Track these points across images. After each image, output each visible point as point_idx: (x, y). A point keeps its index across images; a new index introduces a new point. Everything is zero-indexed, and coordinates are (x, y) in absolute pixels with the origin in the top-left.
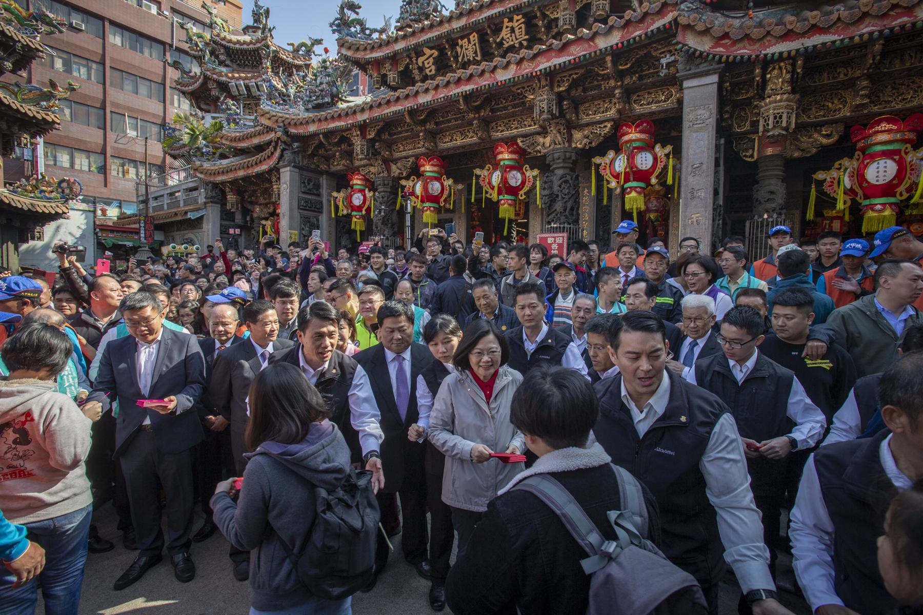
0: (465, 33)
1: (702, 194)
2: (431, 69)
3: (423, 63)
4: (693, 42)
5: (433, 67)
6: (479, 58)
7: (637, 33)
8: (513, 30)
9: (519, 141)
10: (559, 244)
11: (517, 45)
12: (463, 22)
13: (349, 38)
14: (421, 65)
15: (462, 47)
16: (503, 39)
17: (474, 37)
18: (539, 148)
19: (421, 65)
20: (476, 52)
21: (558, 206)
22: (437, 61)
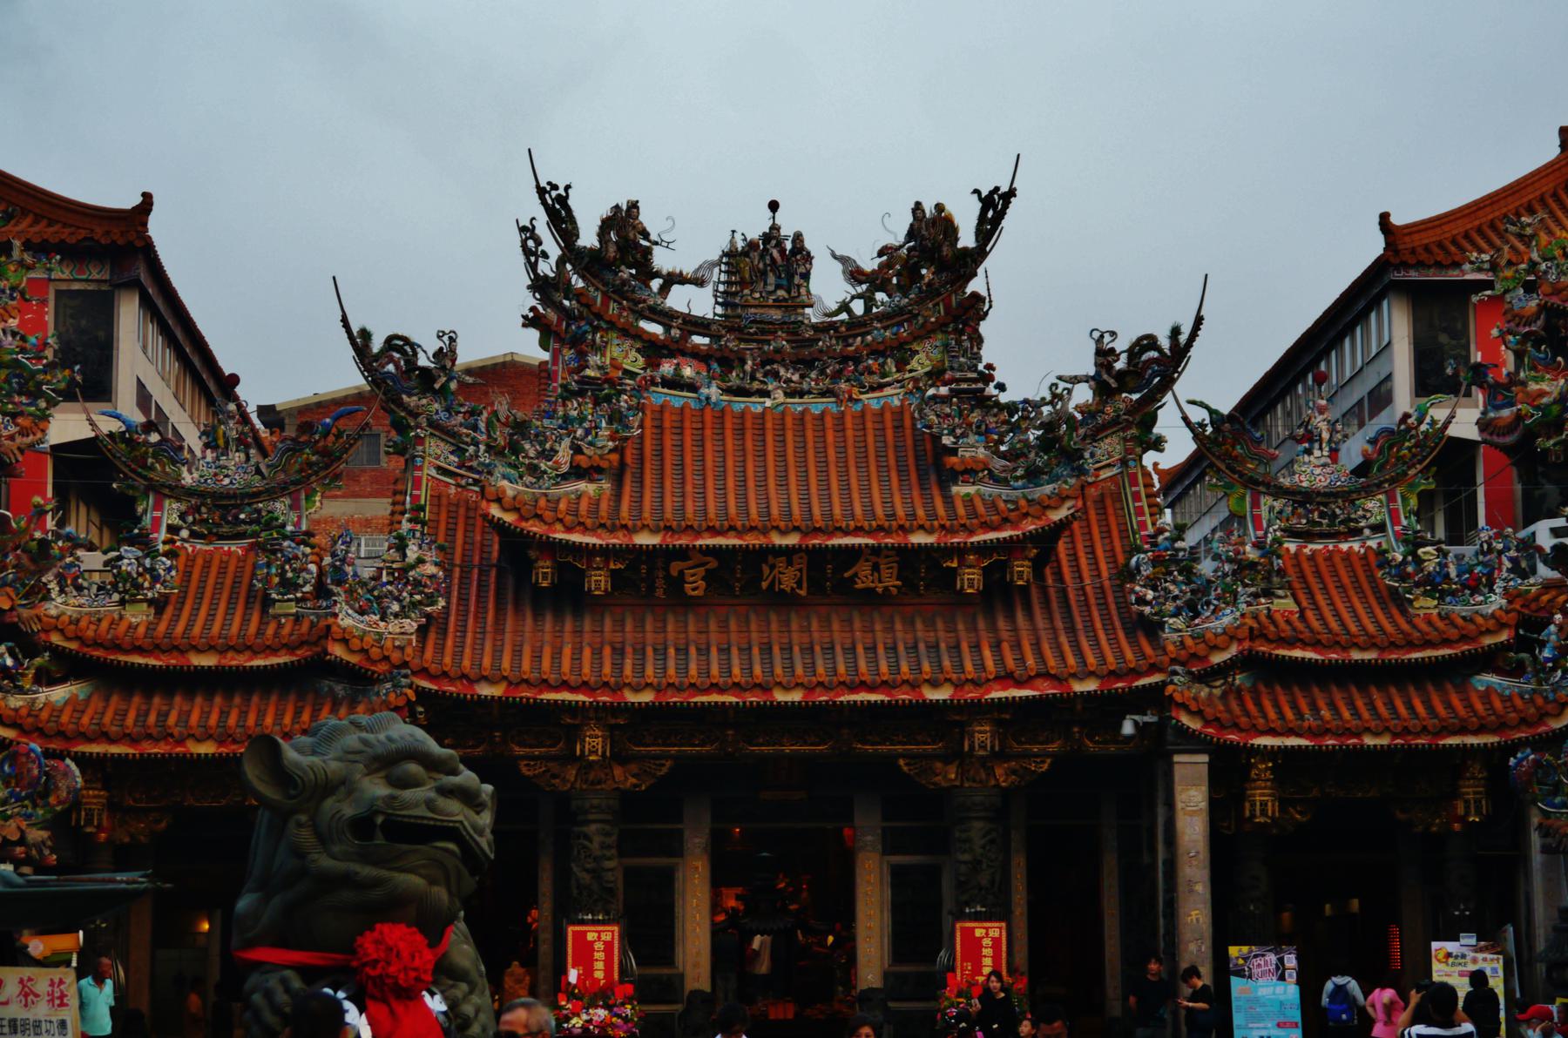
0: (788, 552)
1: (1199, 888)
2: (695, 585)
3: (681, 573)
4: (1185, 720)
5: (702, 583)
6: (803, 593)
7: (1120, 685)
8: (876, 568)
9: (901, 762)
10: (993, 939)
11: (880, 590)
12: (792, 540)
13: (505, 483)
14: (674, 573)
15: (772, 567)
16: (856, 575)
17: (801, 562)
18: (937, 779)
19: (674, 573)
20: (799, 584)
21: (984, 879)
22: (709, 577)
